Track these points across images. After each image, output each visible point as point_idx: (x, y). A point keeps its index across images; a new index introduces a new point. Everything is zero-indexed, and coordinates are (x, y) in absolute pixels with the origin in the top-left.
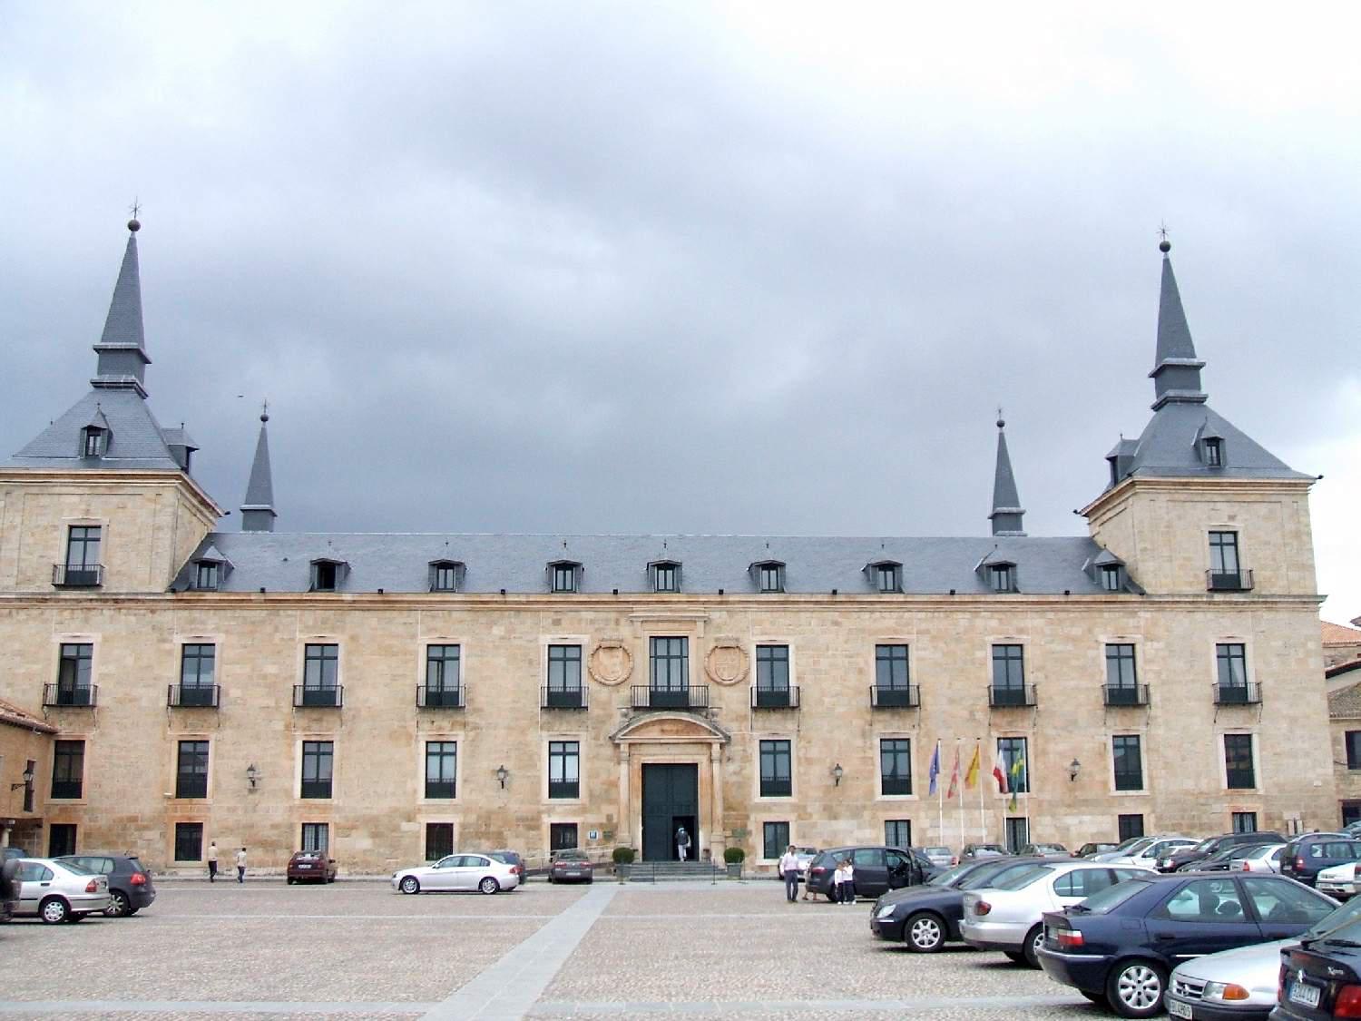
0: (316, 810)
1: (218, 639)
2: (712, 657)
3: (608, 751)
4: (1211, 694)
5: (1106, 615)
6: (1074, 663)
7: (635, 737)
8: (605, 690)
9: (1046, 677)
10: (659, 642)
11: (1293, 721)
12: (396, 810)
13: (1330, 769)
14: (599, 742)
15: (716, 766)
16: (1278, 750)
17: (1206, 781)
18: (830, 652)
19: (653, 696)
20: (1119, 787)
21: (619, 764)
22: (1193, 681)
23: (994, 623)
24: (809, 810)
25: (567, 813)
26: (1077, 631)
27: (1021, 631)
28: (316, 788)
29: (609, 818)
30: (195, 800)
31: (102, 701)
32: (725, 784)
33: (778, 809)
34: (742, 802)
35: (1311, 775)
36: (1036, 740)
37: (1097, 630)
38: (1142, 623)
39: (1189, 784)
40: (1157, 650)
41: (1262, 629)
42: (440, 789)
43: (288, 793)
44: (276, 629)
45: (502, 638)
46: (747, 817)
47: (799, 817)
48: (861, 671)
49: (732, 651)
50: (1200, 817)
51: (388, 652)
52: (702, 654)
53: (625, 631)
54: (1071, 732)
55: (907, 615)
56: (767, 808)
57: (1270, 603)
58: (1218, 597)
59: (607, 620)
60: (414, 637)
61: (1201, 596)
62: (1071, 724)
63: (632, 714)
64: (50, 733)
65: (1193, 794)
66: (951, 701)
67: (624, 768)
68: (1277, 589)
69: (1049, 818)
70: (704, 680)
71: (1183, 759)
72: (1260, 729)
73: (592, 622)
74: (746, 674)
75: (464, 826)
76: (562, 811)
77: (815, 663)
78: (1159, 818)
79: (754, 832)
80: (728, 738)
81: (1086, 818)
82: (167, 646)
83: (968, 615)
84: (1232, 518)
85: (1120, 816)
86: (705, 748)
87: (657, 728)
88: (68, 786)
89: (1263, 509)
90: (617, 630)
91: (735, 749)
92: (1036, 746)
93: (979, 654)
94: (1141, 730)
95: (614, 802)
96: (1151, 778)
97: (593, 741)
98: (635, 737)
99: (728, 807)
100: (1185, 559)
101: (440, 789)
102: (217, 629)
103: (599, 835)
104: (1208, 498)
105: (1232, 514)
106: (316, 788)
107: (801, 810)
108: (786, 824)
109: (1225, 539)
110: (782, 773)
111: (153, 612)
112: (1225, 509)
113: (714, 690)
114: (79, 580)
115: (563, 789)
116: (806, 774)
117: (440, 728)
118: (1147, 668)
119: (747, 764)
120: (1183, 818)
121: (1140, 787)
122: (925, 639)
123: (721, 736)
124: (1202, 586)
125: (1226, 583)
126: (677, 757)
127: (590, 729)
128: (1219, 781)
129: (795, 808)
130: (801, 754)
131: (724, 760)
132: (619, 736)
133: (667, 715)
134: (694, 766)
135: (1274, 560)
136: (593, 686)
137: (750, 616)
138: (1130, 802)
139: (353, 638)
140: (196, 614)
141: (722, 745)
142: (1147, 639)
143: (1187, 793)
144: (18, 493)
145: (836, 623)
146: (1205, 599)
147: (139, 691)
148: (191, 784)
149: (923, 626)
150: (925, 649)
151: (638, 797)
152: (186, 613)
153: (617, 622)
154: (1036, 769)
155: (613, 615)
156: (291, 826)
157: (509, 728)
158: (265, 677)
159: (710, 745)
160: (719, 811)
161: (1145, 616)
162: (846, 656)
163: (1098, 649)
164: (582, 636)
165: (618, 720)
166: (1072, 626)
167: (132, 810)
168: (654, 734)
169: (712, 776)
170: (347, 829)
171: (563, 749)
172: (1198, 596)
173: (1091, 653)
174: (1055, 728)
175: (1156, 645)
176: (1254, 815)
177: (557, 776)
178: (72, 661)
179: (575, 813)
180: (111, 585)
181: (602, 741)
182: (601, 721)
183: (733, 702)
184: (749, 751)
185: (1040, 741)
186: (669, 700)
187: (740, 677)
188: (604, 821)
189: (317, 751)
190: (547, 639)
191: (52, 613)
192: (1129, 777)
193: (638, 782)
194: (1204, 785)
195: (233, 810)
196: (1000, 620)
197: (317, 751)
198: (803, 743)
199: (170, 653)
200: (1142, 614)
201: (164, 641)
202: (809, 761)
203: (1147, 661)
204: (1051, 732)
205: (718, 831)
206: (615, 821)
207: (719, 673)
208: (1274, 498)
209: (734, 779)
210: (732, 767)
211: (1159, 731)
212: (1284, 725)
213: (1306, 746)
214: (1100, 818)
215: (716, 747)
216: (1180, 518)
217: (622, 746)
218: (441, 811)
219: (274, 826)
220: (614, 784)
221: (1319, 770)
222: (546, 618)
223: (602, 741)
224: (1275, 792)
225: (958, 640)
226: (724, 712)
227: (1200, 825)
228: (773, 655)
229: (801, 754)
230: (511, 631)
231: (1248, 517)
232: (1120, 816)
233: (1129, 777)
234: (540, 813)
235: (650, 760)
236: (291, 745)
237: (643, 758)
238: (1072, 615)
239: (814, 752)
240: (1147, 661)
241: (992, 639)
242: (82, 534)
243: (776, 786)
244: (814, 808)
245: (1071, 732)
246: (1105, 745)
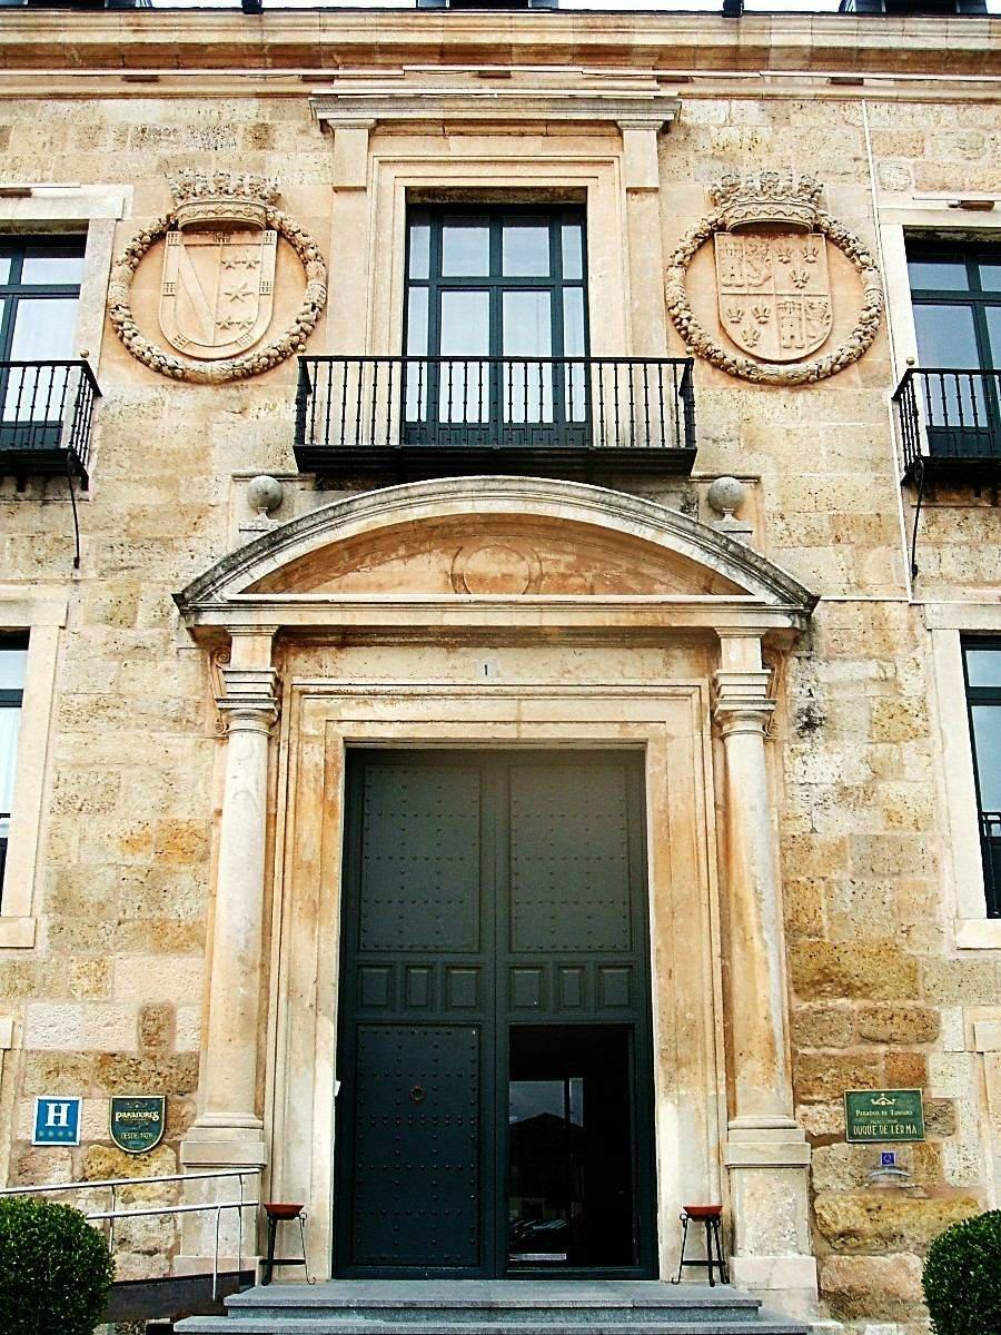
3: (177, 674)
8: (186, 397)
14: (129, 637)
15: (744, 748)
21: (223, 737)
29: (155, 1024)
32: (794, 847)
34: (888, 949)
46: (927, 1030)
49: (792, 243)
52: (653, 255)
63: (303, 501)
67: (247, 745)
74: (871, 329)
79: (965, 1114)
80: (804, 603)
86: (681, 669)
91: (834, 678)
95: (193, 938)
97: (100, 633)
99: (816, 977)
113: (716, 400)
119: (909, 750)
123: (762, 595)
126: (531, 709)
127: (89, 570)
131: (785, 729)
132: (230, 592)
133: (480, 494)
137: (869, 117)
141: (775, 648)
151: (315, 909)
153: (261, 136)
155: (248, 112)
159: (706, 643)
160: (766, 990)
164: (99, 189)
168: (411, 586)
169: (724, 808)
181: (143, 632)
182: (143, 540)
184: (912, 685)
187: (842, 345)
188: (126, 1040)
193: (320, 834)
205: (765, 1093)
206: (184, 1043)
207: (731, 328)
209: (840, 824)
210: (826, 763)
215: (741, 656)
217: (239, 646)
223: (143, 632)
226: (771, 503)
235: (388, 723)
237: (353, 711)
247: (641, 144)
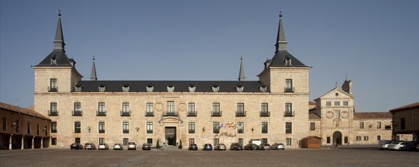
0: (102, 135)
4: (283, 114)
11: (301, 120)
13: (308, 130)
26: (255, 100)
27: (244, 100)
28: (102, 131)
31: (59, 114)
33: (192, 136)
39: (278, 132)
42: (126, 131)
51: (115, 104)
53: (162, 100)
57: (298, 94)
62: (253, 119)
68: (300, 91)
73: (156, 98)
76: (150, 136)
99: (182, 136)
101: (126, 131)
106: (102, 131)
107: (197, 137)
109: (290, 81)
110: (193, 129)
112: (290, 74)
113: (180, 112)
114: (54, 90)
115: (150, 132)
116: (198, 129)
124: (283, 91)
125: (289, 90)
136: (156, 111)
138: (265, 136)
148: (78, 131)
161: (270, 97)
165: (160, 118)
168: (167, 121)
170: (108, 139)
171: (150, 123)
177: (148, 129)
178: (53, 104)
180: (59, 90)
183: (183, 115)
189: (102, 124)
190: (146, 102)
191: (48, 96)
192: (265, 131)
194: (281, 132)
197: (102, 124)
211: (272, 121)
212: (299, 121)
218: (126, 136)
228: (192, 104)
233: (265, 131)
241: (237, 102)
242: (53, 80)
243: (192, 132)
244: (199, 136)
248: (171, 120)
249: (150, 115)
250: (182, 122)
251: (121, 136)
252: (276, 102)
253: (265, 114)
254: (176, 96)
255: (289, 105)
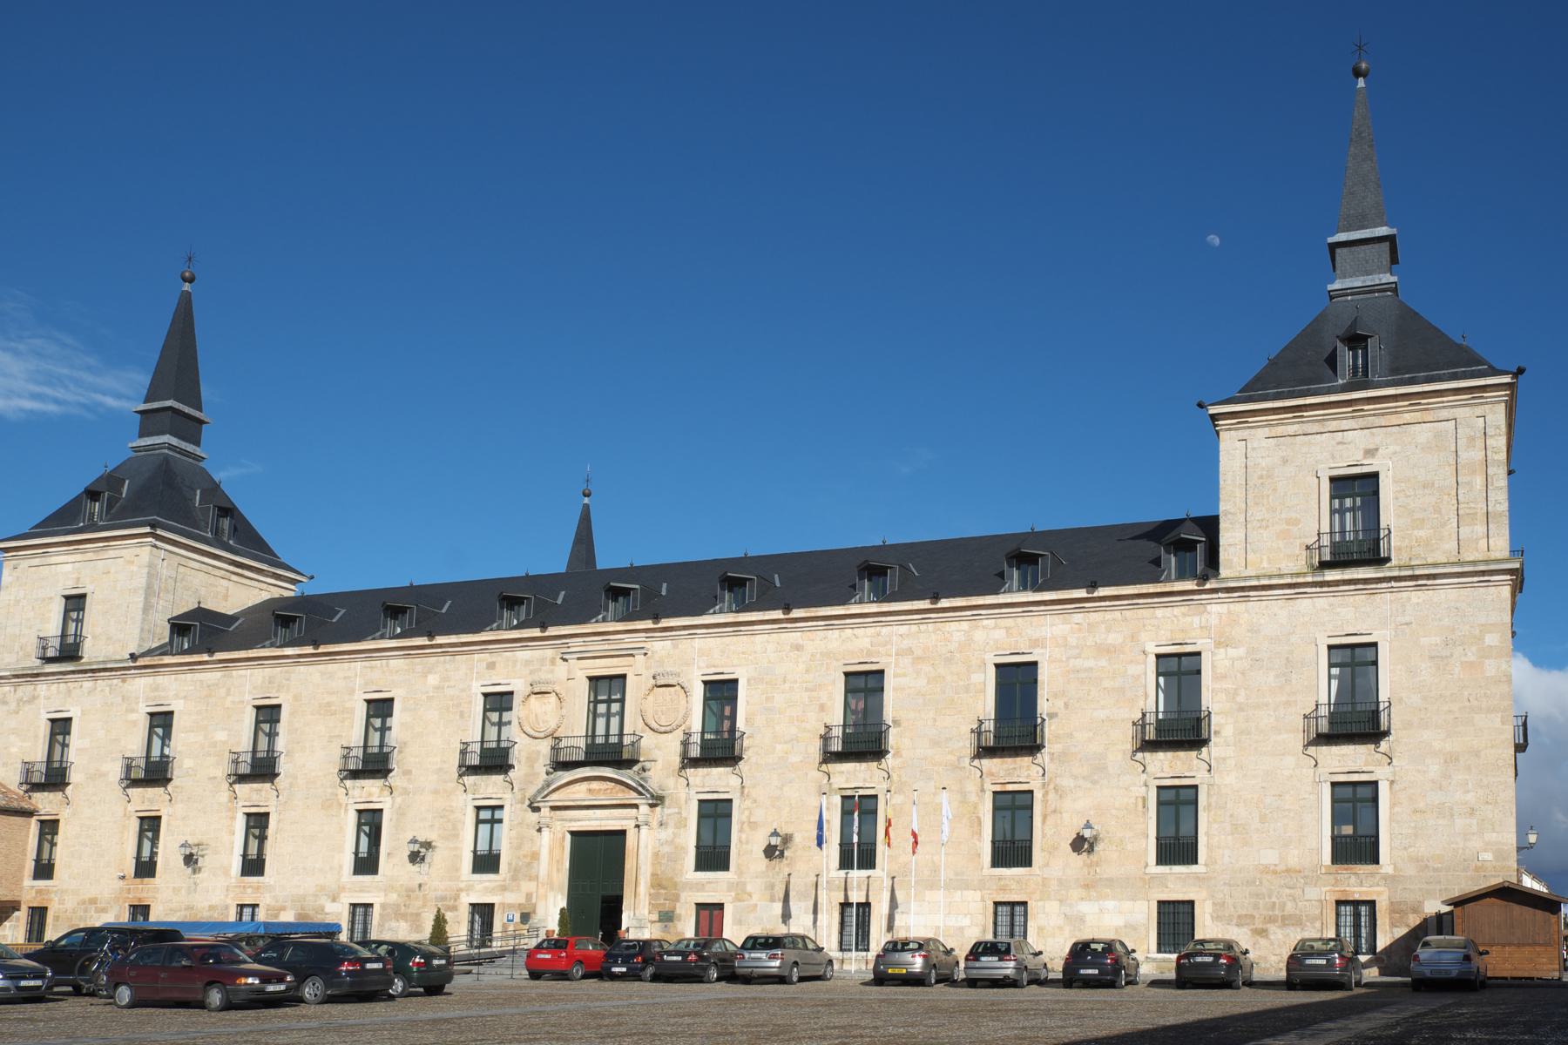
1: (176, 706)
2: (651, 698)
5: (1160, 612)
6: (1106, 684)
7: (557, 798)
9: (1066, 705)
10: (600, 683)
12: (322, 888)
15: (644, 829)
16: (1421, 805)
17: (1296, 852)
18: (787, 686)
19: (591, 748)
20: (1161, 860)
22: (1288, 704)
23: (999, 634)
24: (749, 888)
25: (487, 890)
26: (1114, 638)
27: (1036, 643)
29: (529, 896)
30: (146, 880)
35: (1475, 843)
36: (1046, 794)
37: (1143, 636)
38: (1214, 621)
39: (1270, 857)
40: (1233, 660)
41: (1407, 619)
43: (226, 872)
44: (228, 694)
45: (437, 688)
46: (676, 898)
47: (738, 899)
48: (822, 708)
50: (1283, 906)
54: (1094, 782)
55: (885, 630)
56: (700, 887)
57: (1420, 578)
58: (1332, 575)
59: (543, 660)
60: (352, 692)
61: (1304, 574)
64: (28, 814)
65: (1275, 872)
66: (935, 743)
68: (1442, 552)
69: (1056, 904)
70: (641, 724)
71: (1263, 819)
72: (1394, 774)
73: (527, 663)
75: (383, 906)
76: (483, 889)
77: (767, 699)
78: (1219, 905)
81: (1110, 904)
82: (133, 717)
83: (965, 625)
84: (1370, 453)
85: (1160, 903)
87: (584, 786)
88: (44, 870)
89: (1423, 433)
90: (552, 672)
92: (1045, 802)
93: (977, 678)
94: (1200, 777)
96: (1209, 847)
98: (557, 798)
99: (658, 883)
100: (1288, 521)
102: (177, 696)
103: (517, 918)
104: (1333, 425)
105: (1372, 447)
107: (740, 892)
108: (720, 906)
111: (124, 681)
115: (486, 863)
116: (745, 843)
117: (370, 795)
118: (1217, 686)
120: (1256, 907)
121: (1194, 860)
122: (907, 660)
128: (1320, 851)
129: (731, 886)
130: (744, 818)
134: (623, 833)
135: (1438, 510)
137: (698, 643)
138: (1177, 882)
139: (297, 698)
140: (159, 679)
142: (1218, 644)
143: (1266, 870)
144: (24, 564)
145: (798, 648)
146: (1309, 579)
147: (105, 767)
149: (906, 643)
150: (905, 675)
152: (150, 680)
154: (1044, 836)
155: (549, 653)
156: (227, 907)
157: (436, 792)
158: (214, 745)
161: (1217, 610)
162: (807, 690)
163: (1145, 663)
166: (1109, 630)
167: (92, 892)
168: (579, 793)
171: (489, 815)
172: (1298, 575)
173: (1134, 670)
174: (1075, 778)
175: (1232, 652)
176: (1372, 904)
177: (483, 847)
179: (492, 891)
185: (1051, 796)
186: (610, 755)
188: (523, 901)
191: (42, 688)
192: (1177, 848)
195: (176, 890)
196: (1008, 629)
197: (258, 823)
198: (748, 803)
199: (135, 723)
200: (1214, 608)
201: (133, 711)
202: (753, 825)
203: (1219, 677)
204: (1066, 782)
208: (1444, 414)
209: (666, 849)
210: (665, 834)
212: (1434, 769)
213: (1470, 797)
214: (1127, 905)
215: (644, 809)
216: (1285, 461)
219: (212, 908)
220: (535, 856)
221: (1491, 836)
222: (480, 659)
224: (1410, 871)
225: (949, 660)
227: (1284, 918)
229: (744, 818)
230: (445, 679)
231: (1398, 448)
232: (1160, 903)
233: (1177, 848)
234: (461, 890)
235: (577, 827)
236: (233, 818)
238: (1108, 616)
239: (759, 815)
240: (1219, 677)
245: (1094, 782)
246: (1144, 799)
247: (640, 658)
248: (604, 792)
249: (495, 761)
250: (657, 801)
251: (342, 889)
252: (1262, 648)
253: (1181, 729)
254: (629, 641)
255: (1355, 660)
